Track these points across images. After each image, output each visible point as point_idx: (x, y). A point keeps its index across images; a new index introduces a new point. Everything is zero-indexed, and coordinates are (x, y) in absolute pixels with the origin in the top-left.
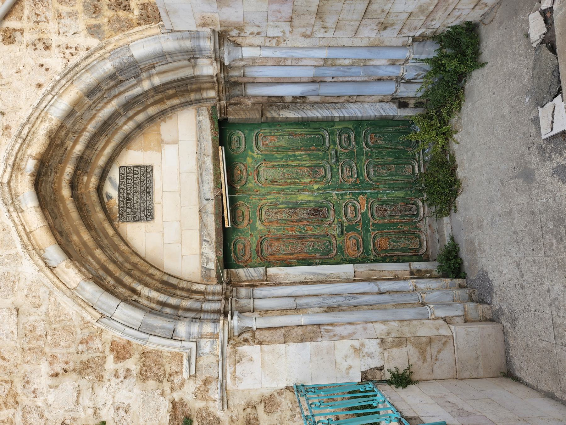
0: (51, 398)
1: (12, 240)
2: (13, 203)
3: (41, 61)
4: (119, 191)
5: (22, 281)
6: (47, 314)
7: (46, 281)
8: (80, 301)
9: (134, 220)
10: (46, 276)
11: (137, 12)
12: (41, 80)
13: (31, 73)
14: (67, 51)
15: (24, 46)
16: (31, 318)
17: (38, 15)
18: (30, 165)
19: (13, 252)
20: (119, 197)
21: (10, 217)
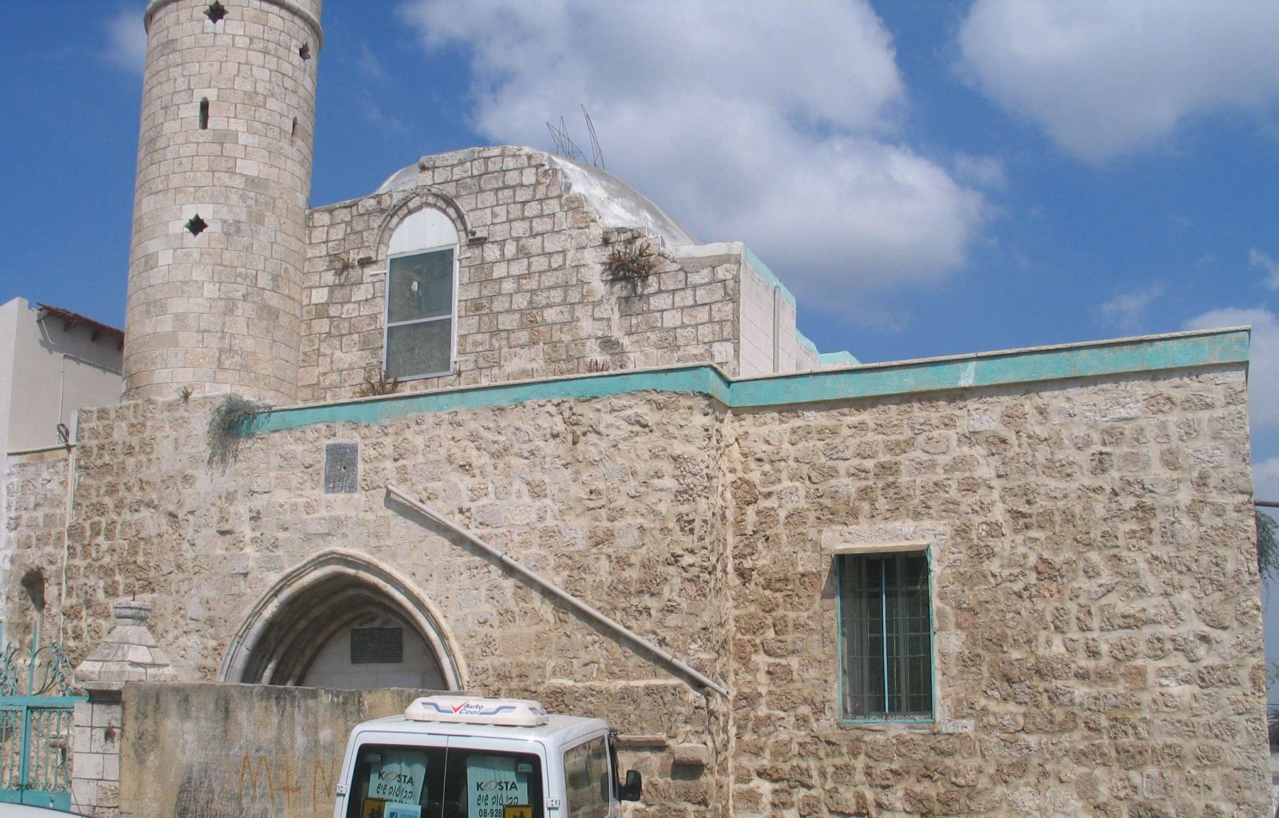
0: (195, 599)
1: (295, 562)
2: (320, 562)
3: (435, 576)
4: (379, 629)
5: (267, 573)
6: (244, 594)
7: (264, 593)
8: (250, 620)
9: (353, 644)
10: (267, 594)
11: (481, 664)
12: (418, 577)
13: (424, 568)
14: (443, 598)
15: (449, 559)
16: (242, 583)
17: (477, 568)
18: (351, 571)
19: (286, 565)
20: (373, 629)
21: (309, 562)
